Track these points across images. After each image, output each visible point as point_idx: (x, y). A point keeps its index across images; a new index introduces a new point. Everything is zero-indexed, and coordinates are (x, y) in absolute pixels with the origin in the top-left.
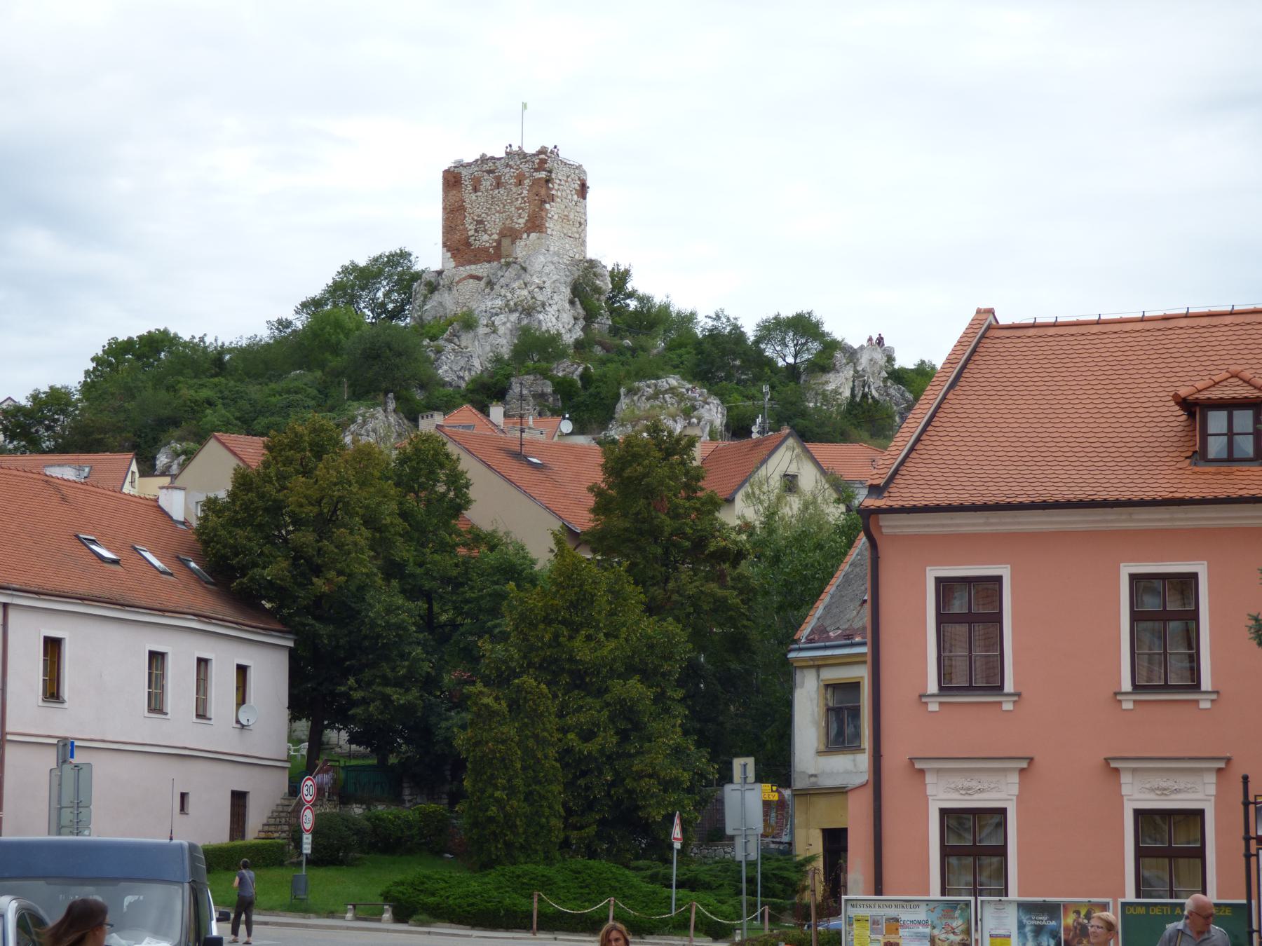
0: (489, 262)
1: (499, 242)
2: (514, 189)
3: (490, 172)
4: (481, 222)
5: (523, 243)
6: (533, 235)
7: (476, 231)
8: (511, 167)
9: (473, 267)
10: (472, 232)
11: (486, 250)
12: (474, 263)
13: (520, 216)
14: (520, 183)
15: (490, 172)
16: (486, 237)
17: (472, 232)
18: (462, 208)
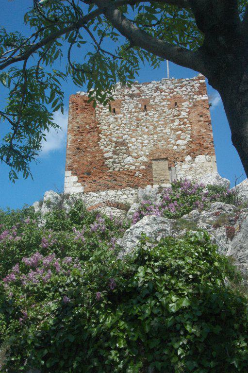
0: (136, 187)
1: (149, 166)
2: (168, 111)
3: (132, 96)
4: (124, 143)
5: (185, 166)
6: (200, 158)
7: (114, 153)
8: (162, 91)
9: (111, 193)
10: (110, 154)
11: (131, 174)
12: (113, 188)
13: (179, 137)
14: (176, 104)
15: (132, 96)
16: (129, 159)
17: (110, 154)
18: (95, 129)
